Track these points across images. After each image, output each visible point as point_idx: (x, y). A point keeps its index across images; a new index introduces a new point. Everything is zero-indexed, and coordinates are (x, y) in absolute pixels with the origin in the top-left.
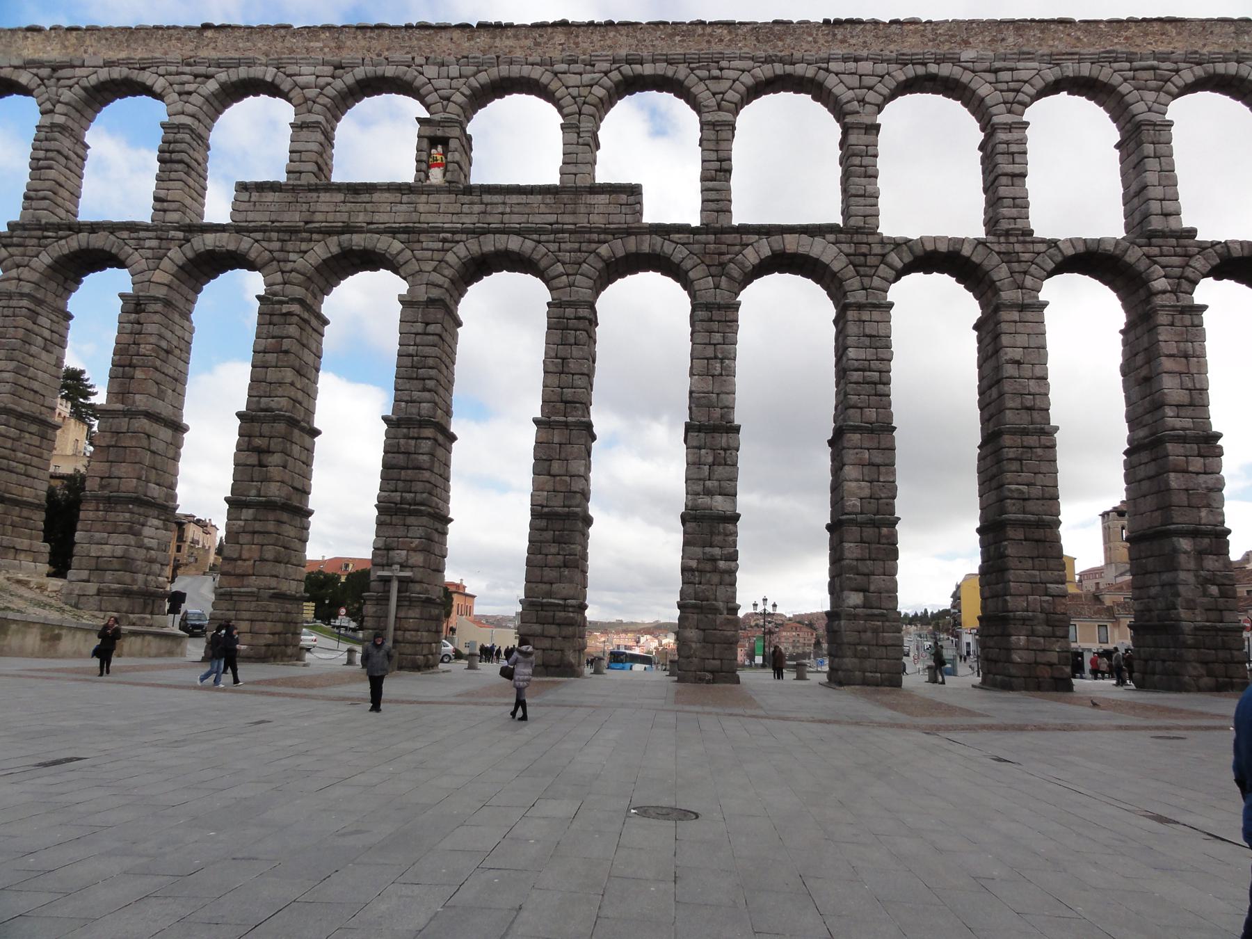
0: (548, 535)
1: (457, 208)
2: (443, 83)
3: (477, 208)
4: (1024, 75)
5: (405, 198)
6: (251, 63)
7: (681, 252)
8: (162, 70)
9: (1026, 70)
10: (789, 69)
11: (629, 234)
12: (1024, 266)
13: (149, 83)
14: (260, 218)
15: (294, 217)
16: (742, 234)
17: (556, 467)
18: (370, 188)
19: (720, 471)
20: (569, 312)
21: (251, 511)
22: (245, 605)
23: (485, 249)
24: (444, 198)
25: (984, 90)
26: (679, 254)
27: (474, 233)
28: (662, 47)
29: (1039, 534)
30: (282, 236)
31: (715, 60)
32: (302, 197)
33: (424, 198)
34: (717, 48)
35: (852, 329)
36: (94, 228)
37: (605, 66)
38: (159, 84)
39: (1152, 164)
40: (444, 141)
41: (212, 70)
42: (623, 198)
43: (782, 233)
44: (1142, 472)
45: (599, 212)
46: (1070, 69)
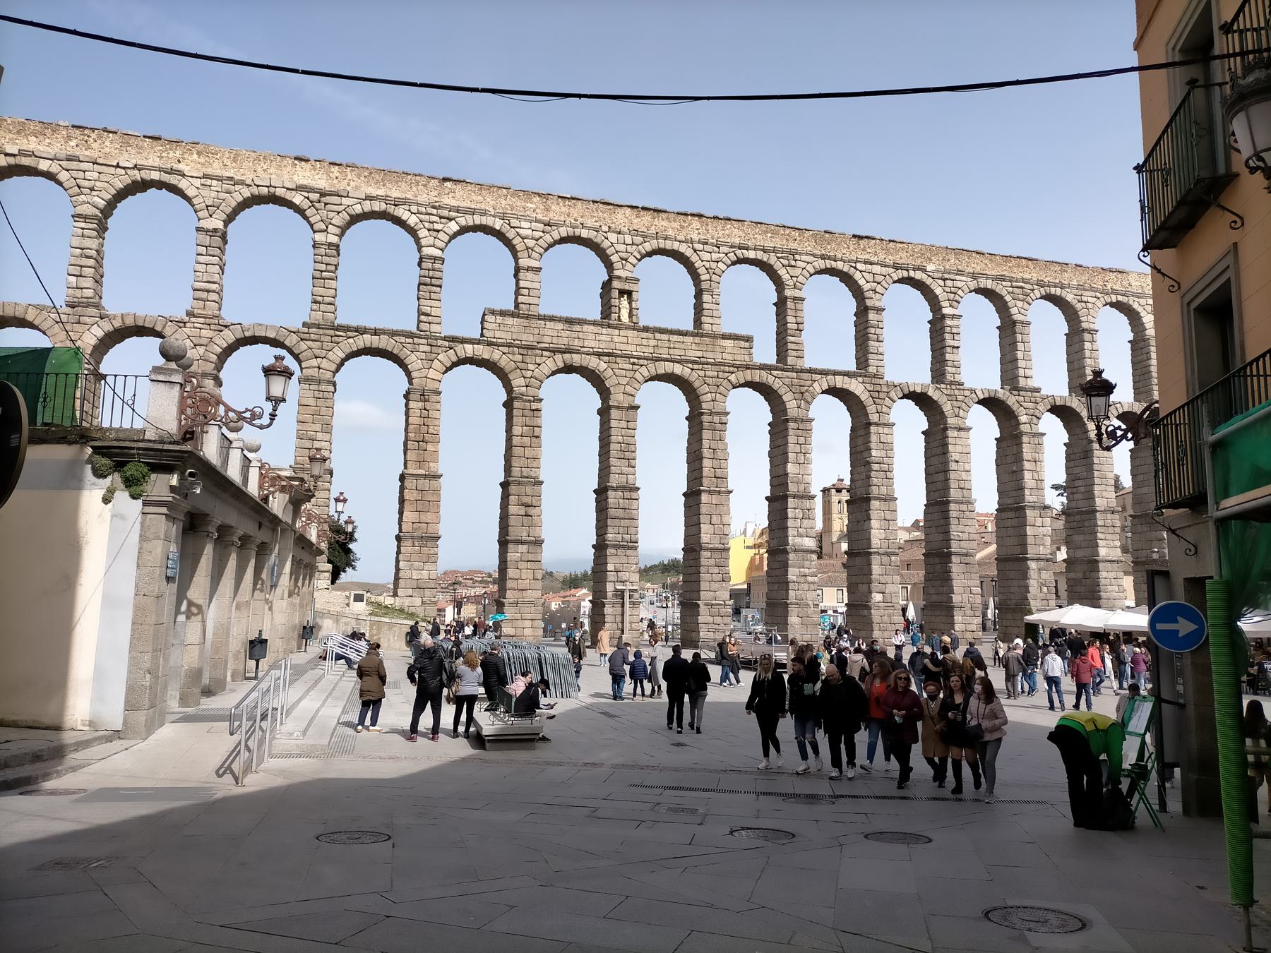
0: (712, 562)
2: (621, 248)
3: (653, 343)
4: (959, 284)
5: (604, 331)
6: (483, 213)
8: (414, 209)
9: (961, 281)
10: (834, 264)
12: (959, 404)
13: (404, 218)
15: (527, 338)
17: (715, 519)
18: (582, 322)
19: (806, 521)
20: (716, 419)
21: (525, 547)
22: (527, 610)
24: (630, 333)
25: (938, 291)
26: (776, 384)
28: (760, 240)
29: (967, 559)
30: (522, 351)
31: (793, 253)
32: (534, 323)
34: (793, 245)
35: (874, 438)
36: (376, 332)
37: (726, 249)
38: (412, 220)
39: (1020, 346)
40: (629, 293)
41: (453, 214)
42: (742, 344)
44: (1009, 523)
46: (984, 283)
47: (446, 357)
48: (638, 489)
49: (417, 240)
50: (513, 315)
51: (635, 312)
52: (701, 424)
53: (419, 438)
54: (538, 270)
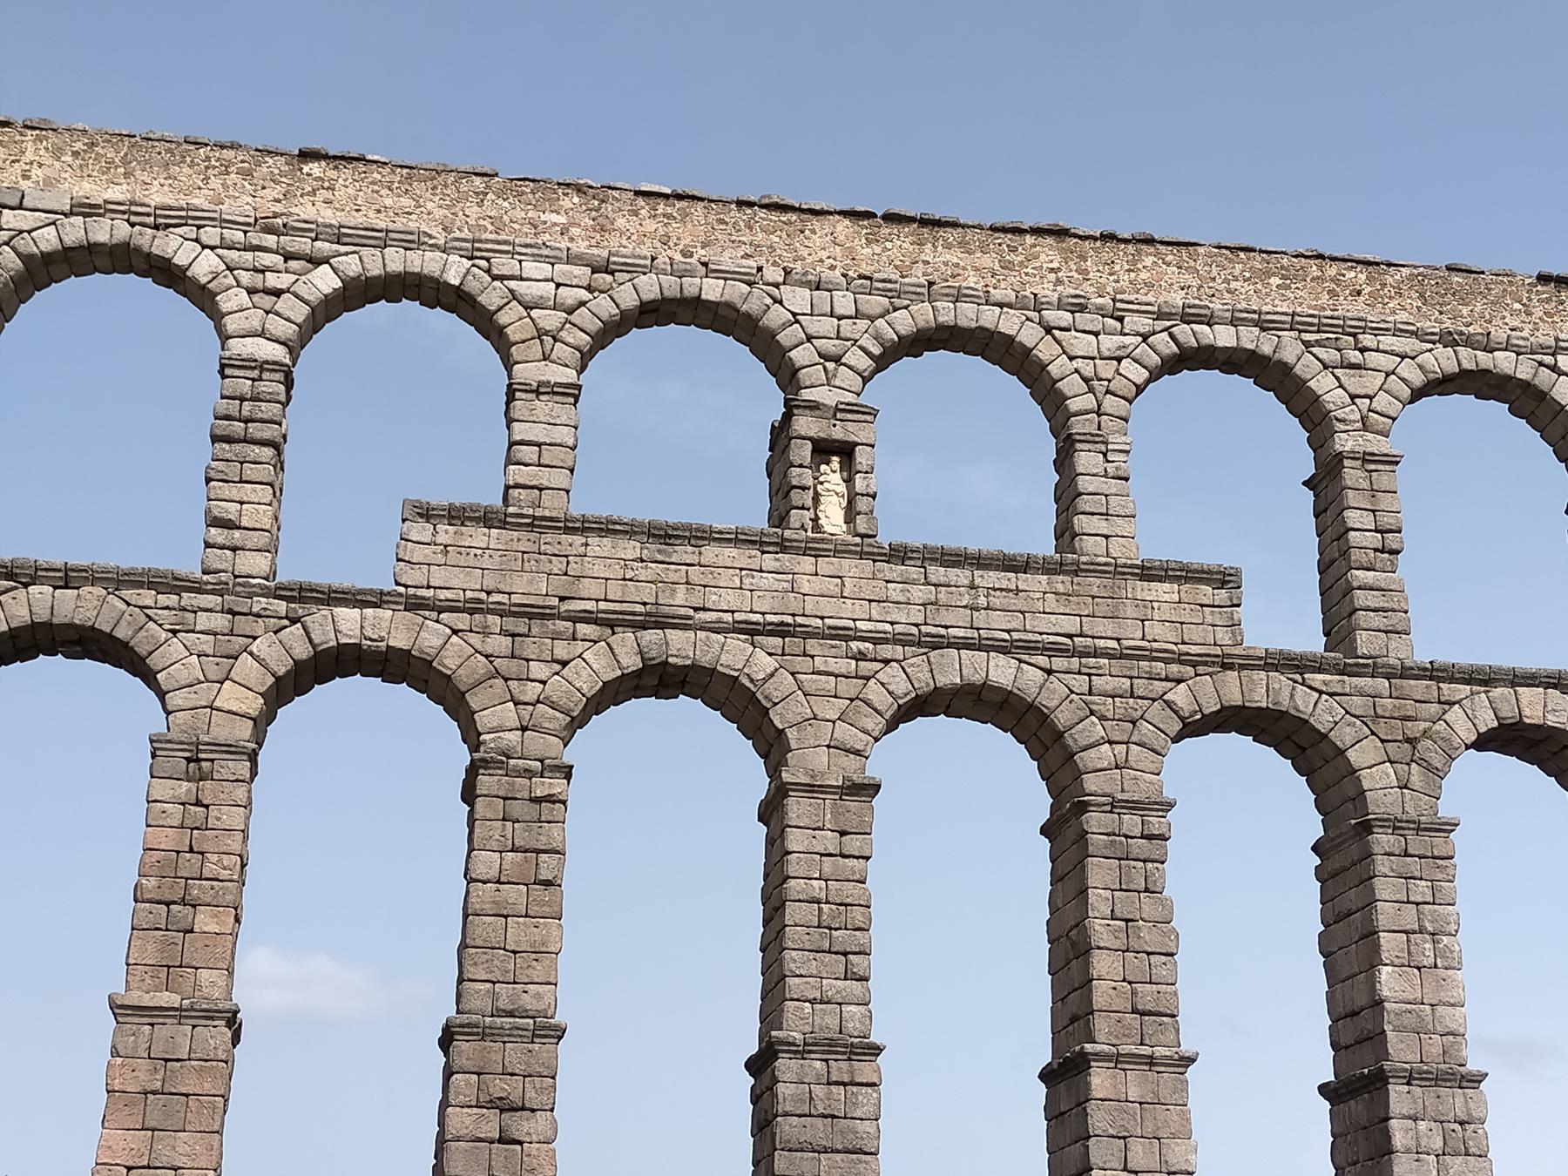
1: (875, 589)
3: (920, 593)
5: (769, 561)
7: (1330, 711)
11: (1226, 667)
14: (455, 582)
15: (530, 586)
16: (1439, 680)
18: (700, 536)
23: (943, 680)
24: (849, 566)
27: (919, 644)
30: (511, 624)
32: (552, 541)
33: (807, 563)
40: (846, 451)
42: (1206, 592)
43: (1513, 685)
45: (1163, 614)
47: (277, 649)
48: (876, 1050)
49: (216, 316)
50: (488, 519)
51: (862, 504)
52: (1086, 838)
53: (185, 896)
54: (572, 393)
